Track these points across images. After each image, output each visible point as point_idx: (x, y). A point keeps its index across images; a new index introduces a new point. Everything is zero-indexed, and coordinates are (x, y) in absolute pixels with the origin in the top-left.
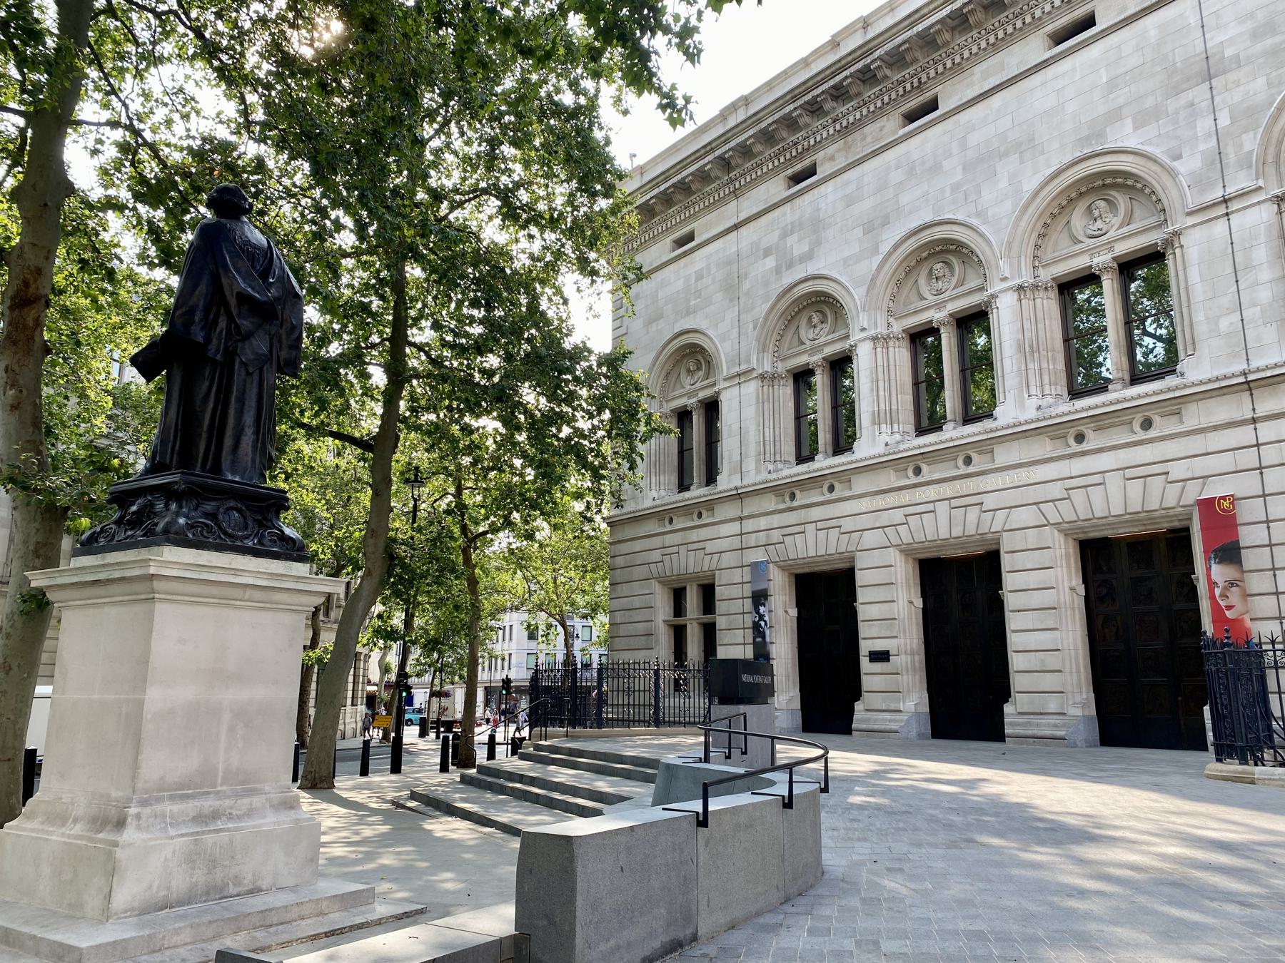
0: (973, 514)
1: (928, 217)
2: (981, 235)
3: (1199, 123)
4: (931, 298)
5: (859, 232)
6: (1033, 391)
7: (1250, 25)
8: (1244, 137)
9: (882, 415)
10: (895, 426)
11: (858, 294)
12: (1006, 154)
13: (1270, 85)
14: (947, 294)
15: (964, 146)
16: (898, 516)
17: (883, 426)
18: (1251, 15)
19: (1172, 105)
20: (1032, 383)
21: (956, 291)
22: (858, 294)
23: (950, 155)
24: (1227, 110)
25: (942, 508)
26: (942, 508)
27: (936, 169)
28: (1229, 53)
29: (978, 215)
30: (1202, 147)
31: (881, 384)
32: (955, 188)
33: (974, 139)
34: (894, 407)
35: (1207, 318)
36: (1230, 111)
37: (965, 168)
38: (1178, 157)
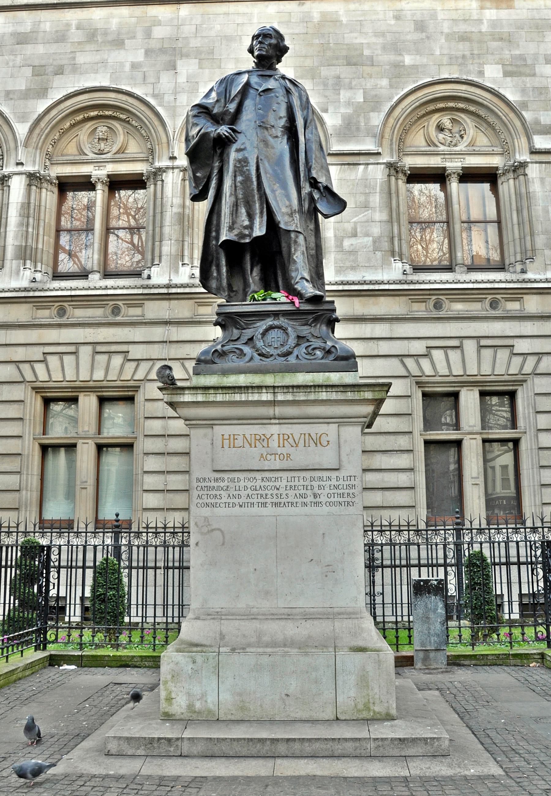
0: (117, 361)
1: (106, 83)
2: (157, 115)
3: (342, 92)
4: (91, 156)
5: (28, 72)
6: (186, 261)
7: (381, 40)
8: (372, 114)
9: (28, 252)
10: (39, 265)
11: (22, 130)
12: (187, 56)
13: (391, 86)
14: (109, 155)
15: (148, 34)
16: (36, 353)
17: (28, 262)
18: (383, 34)
19: (325, 72)
20: (186, 253)
21: (117, 156)
22: (22, 130)
23: (134, 37)
24: (362, 91)
25: (85, 352)
26: (85, 352)
27: (118, 43)
28: (367, 52)
29: (154, 96)
30: (343, 110)
31: (31, 220)
32: (135, 66)
33: (159, 32)
34: (40, 246)
35: (335, 236)
36: (364, 93)
37: (148, 52)
38: (326, 111)
